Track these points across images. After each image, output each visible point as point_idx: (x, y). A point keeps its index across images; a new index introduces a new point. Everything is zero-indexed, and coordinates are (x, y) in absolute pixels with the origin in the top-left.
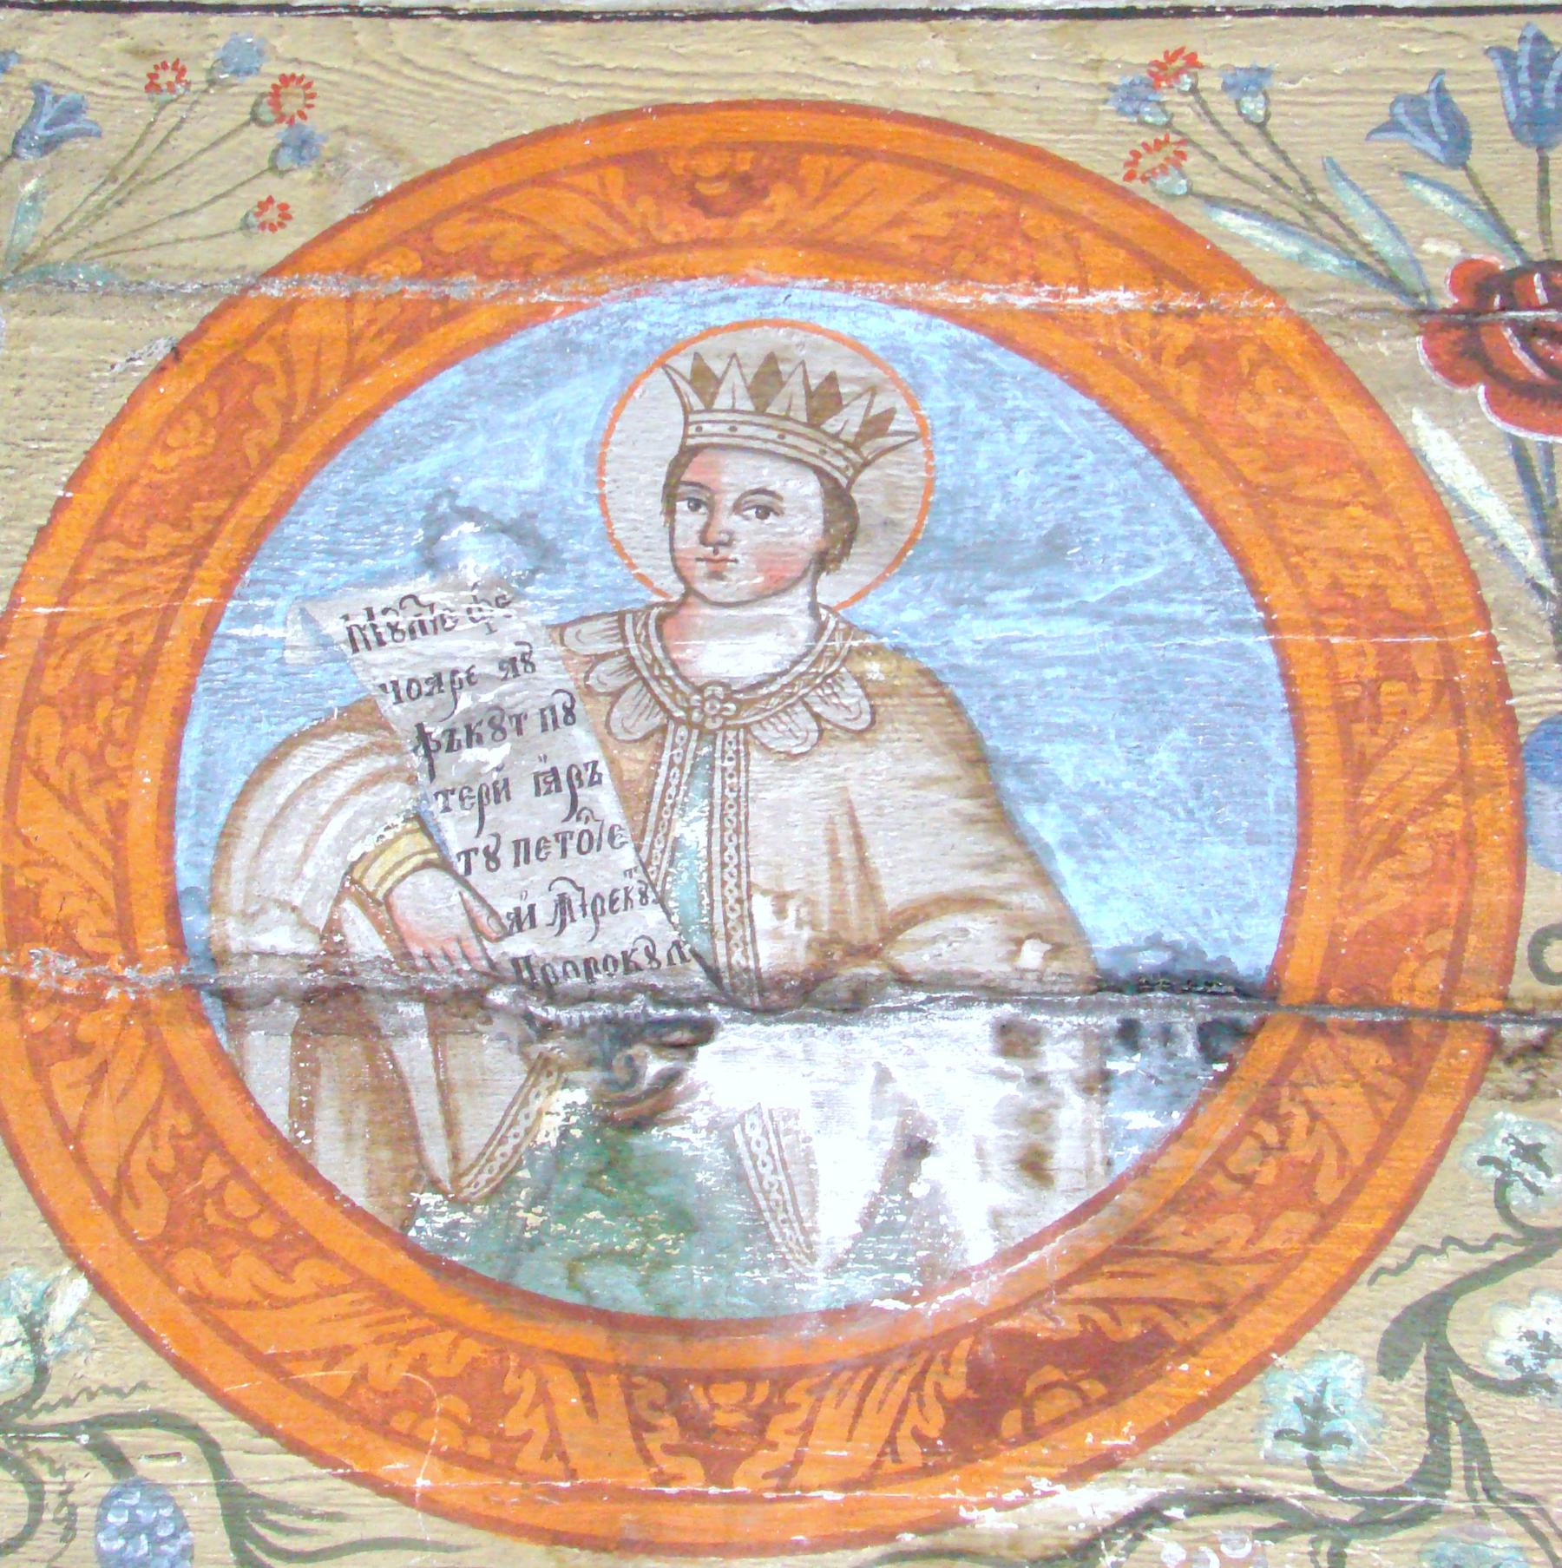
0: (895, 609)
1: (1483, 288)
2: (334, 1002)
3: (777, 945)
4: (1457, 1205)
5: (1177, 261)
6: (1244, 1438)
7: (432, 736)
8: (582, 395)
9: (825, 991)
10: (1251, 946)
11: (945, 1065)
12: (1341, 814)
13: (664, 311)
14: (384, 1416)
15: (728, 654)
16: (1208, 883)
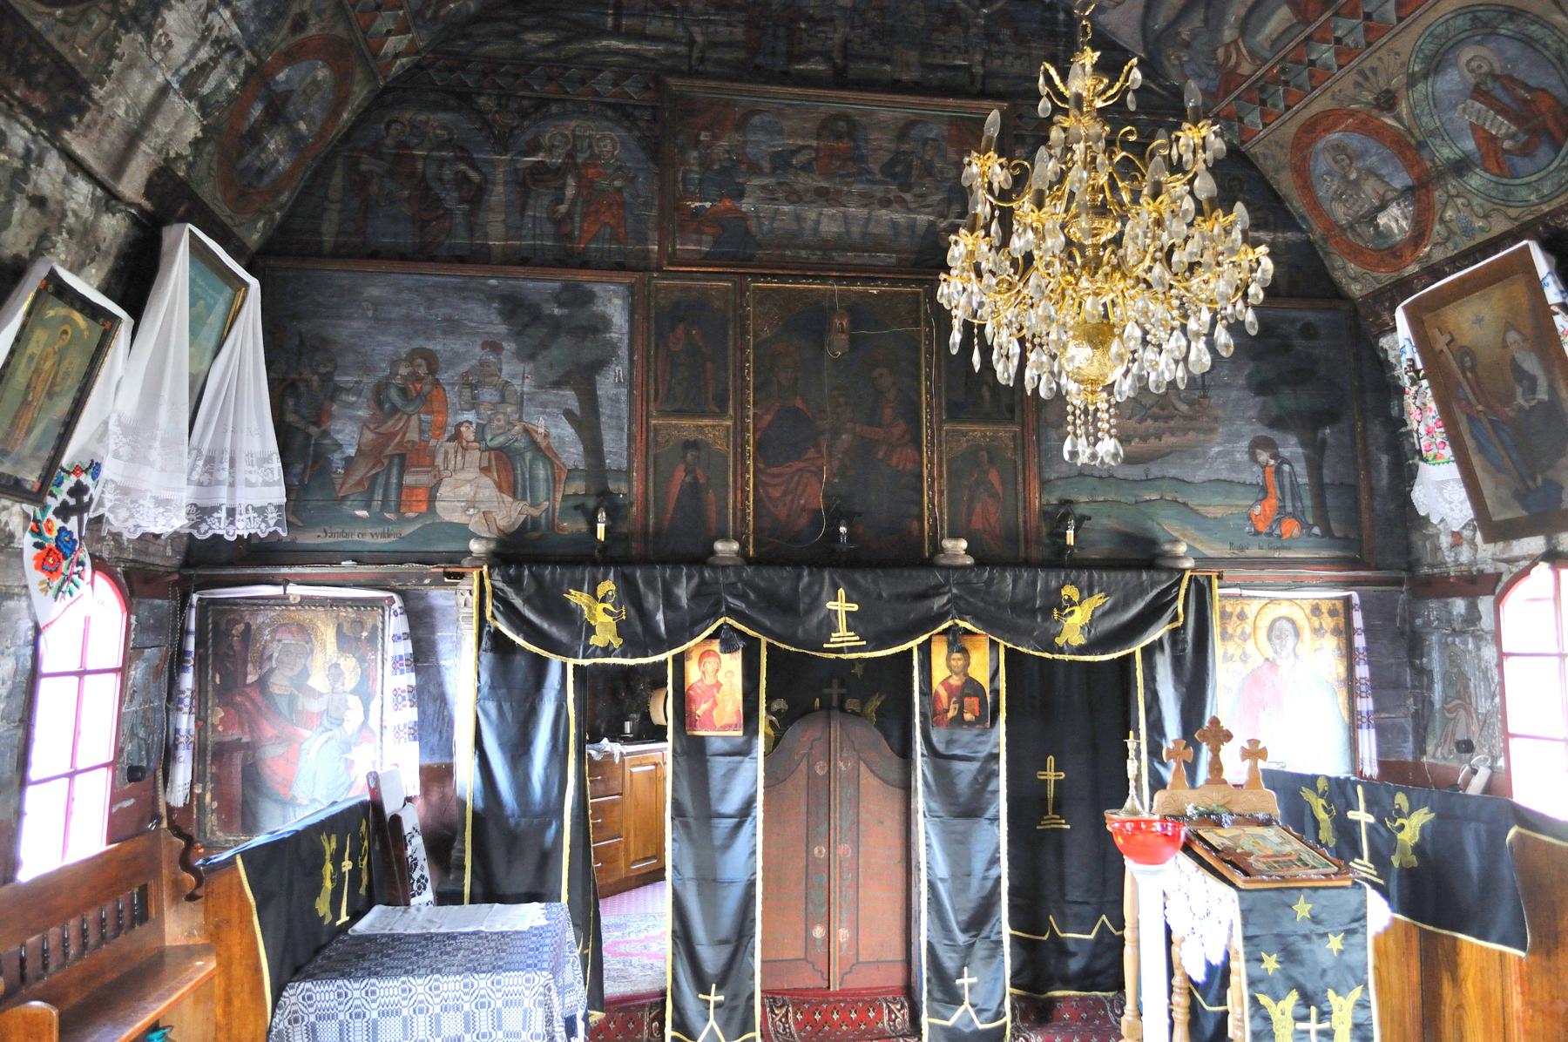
0: (1360, 164)
1: (1377, 99)
2: (1351, 226)
3: (1376, 202)
4: (1438, 206)
5: (1352, 114)
6: (1435, 238)
7: (1338, 197)
8: (1321, 158)
9: (1383, 207)
10: (1409, 182)
11: (1394, 210)
12: (1409, 166)
13: (1320, 145)
14: (1378, 266)
15: (1353, 176)
16: (1401, 180)
